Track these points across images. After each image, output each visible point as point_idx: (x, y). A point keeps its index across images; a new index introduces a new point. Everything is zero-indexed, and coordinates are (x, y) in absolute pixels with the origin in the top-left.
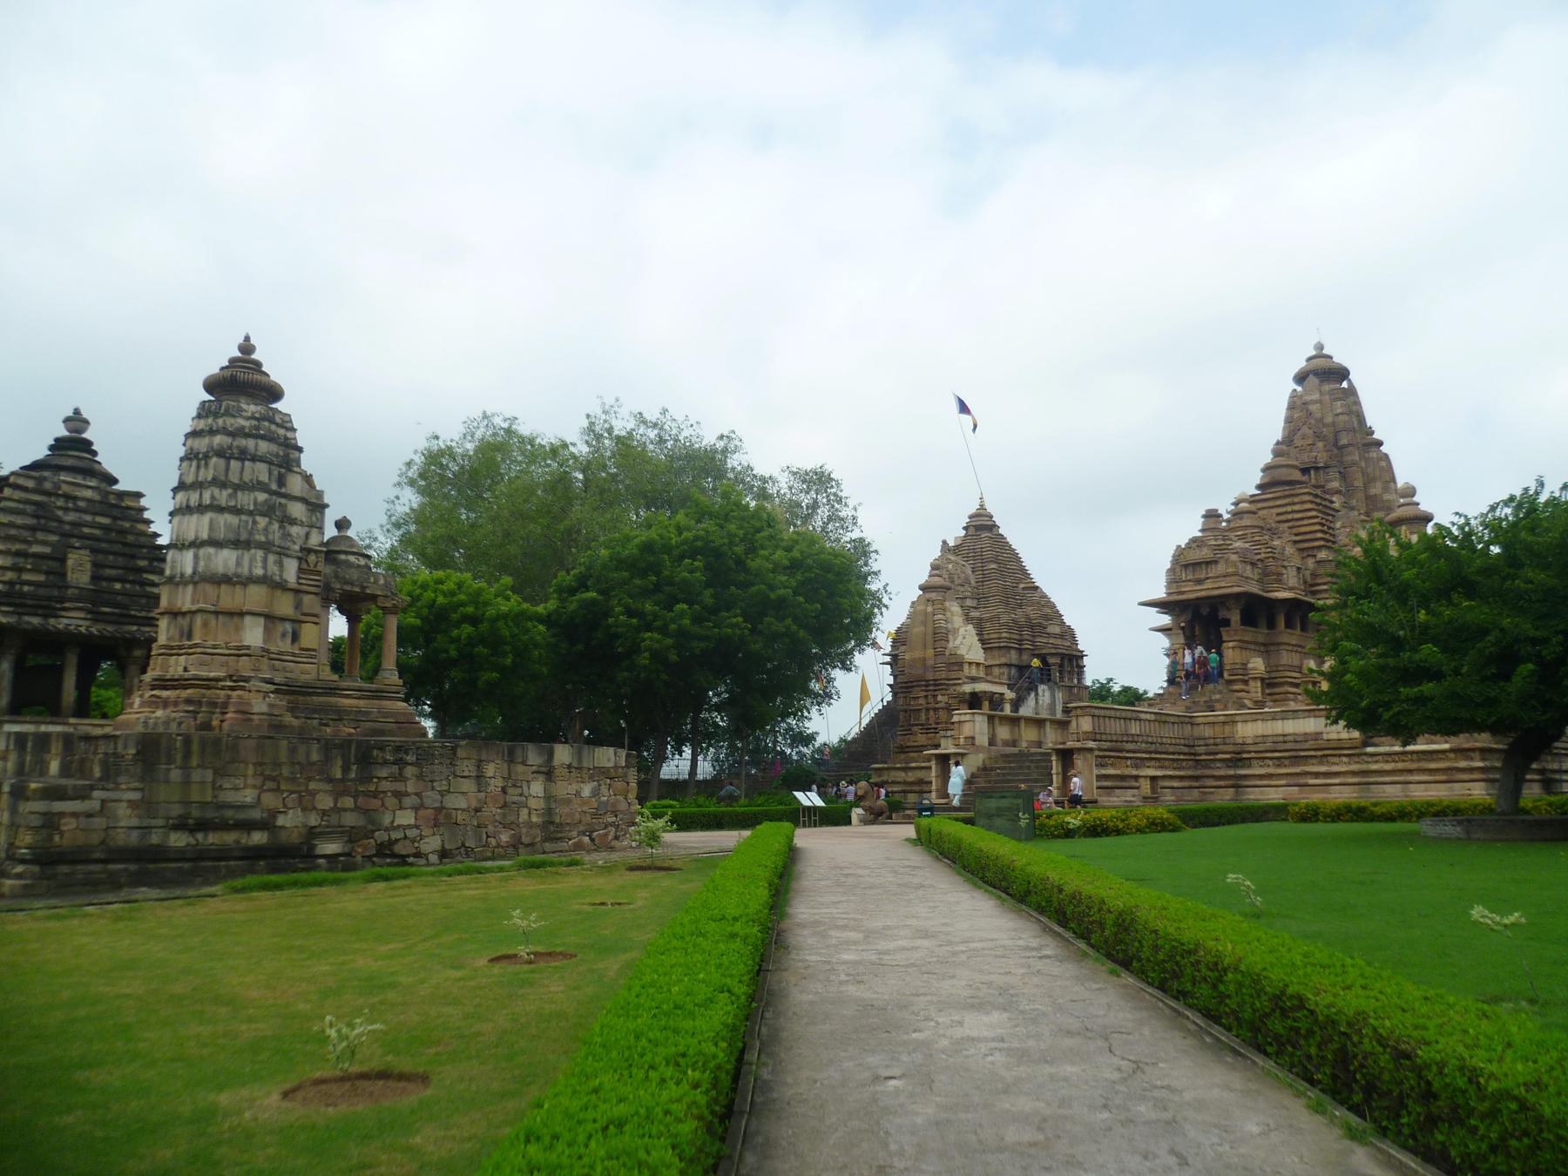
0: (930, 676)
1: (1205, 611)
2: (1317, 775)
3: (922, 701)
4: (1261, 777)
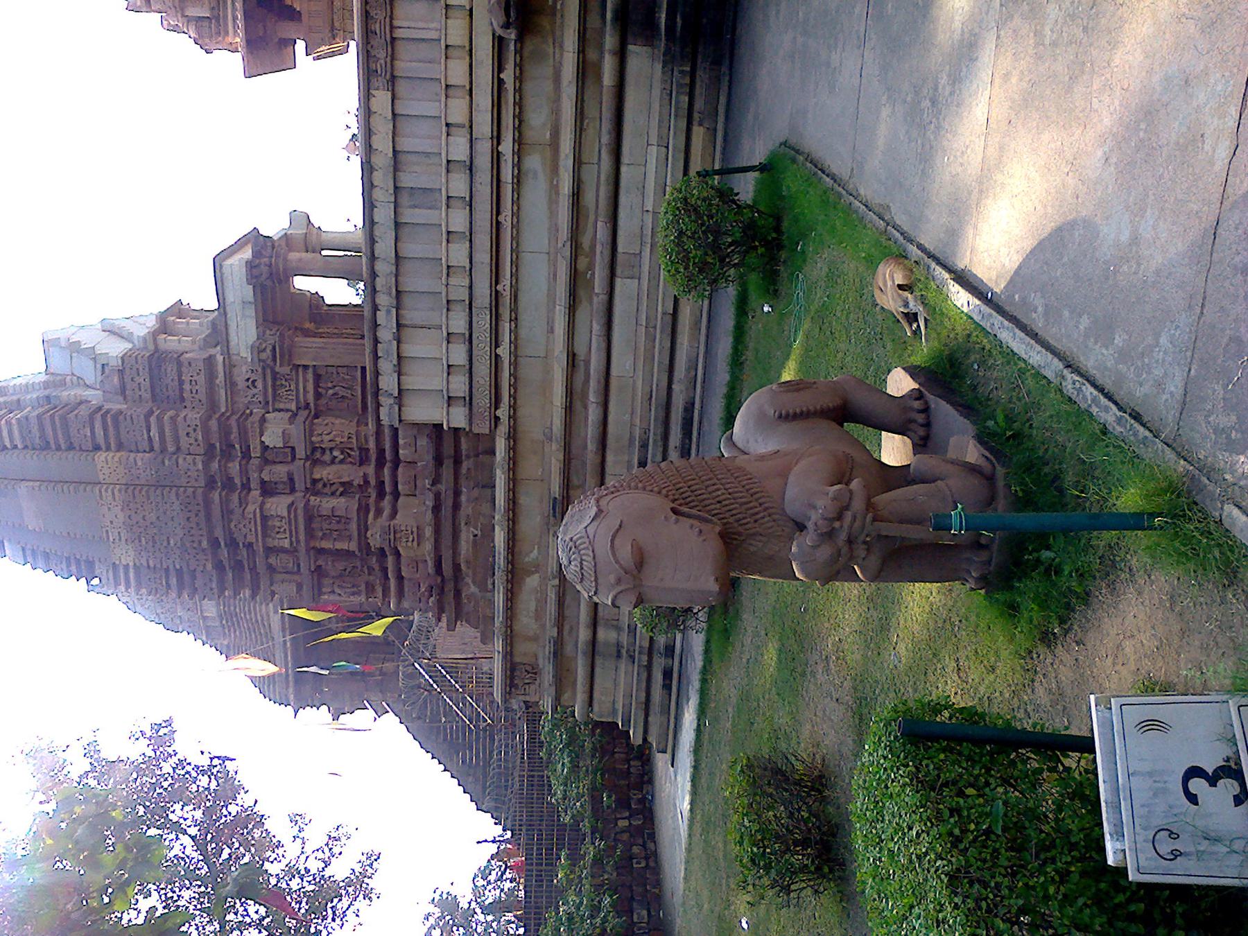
3: (278, 505)
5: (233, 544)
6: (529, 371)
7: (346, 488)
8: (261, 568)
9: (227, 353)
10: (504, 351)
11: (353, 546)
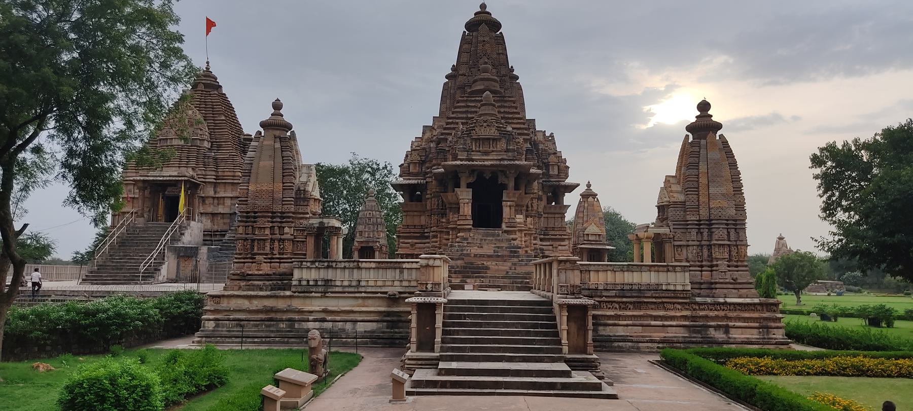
0: (278, 208)
1: (487, 176)
2: (656, 318)
3: (267, 232)
4: (610, 317)
5: (255, 217)
6: (308, 301)
7: (272, 249)
8: (247, 224)
9: (309, 218)
10: (313, 294)
11: (255, 251)
